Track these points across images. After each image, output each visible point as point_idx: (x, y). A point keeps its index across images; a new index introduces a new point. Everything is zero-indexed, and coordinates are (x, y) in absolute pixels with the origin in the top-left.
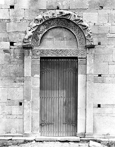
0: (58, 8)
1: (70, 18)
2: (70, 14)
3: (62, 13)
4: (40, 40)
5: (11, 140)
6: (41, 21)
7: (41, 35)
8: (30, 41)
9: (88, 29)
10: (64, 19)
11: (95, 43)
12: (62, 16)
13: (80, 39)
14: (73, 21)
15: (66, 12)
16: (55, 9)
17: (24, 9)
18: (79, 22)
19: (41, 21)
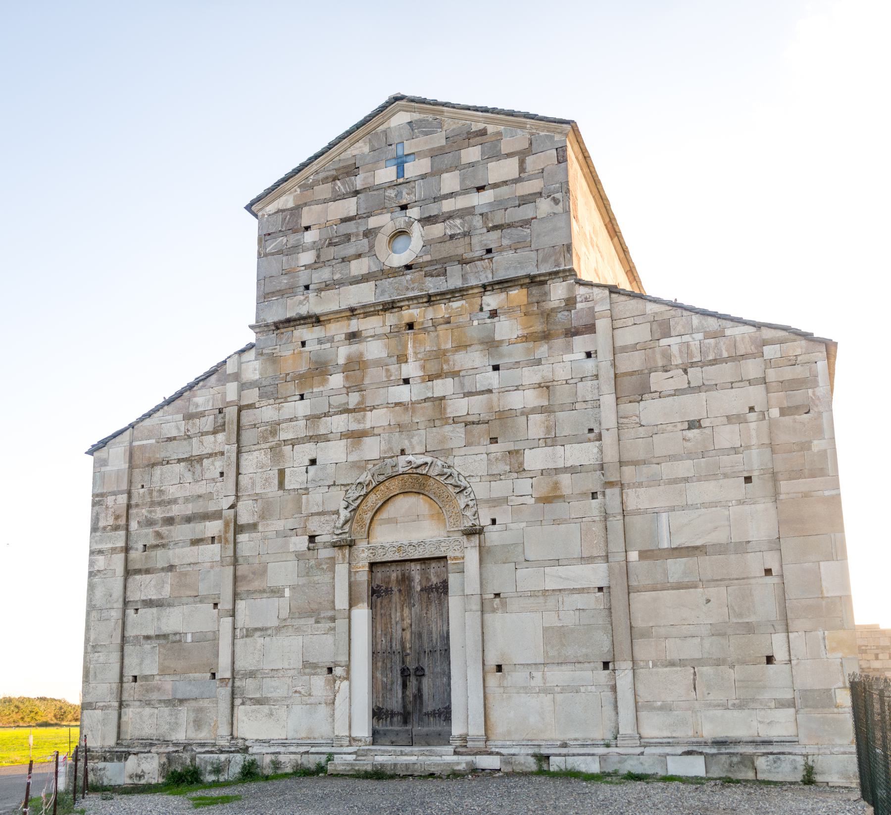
0: (403, 452)
1: (427, 472)
2: (426, 463)
3: (410, 462)
4: (368, 525)
5: (307, 753)
6: (368, 485)
7: (370, 514)
8: (347, 530)
9: (466, 493)
10: (417, 473)
11: (485, 521)
12: (411, 468)
13: (451, 514)
14: (435, 477)
15: (420, 460)
16: (397, 456)
17: (336, 463)
18: (445, 479)
19: (368, 485)
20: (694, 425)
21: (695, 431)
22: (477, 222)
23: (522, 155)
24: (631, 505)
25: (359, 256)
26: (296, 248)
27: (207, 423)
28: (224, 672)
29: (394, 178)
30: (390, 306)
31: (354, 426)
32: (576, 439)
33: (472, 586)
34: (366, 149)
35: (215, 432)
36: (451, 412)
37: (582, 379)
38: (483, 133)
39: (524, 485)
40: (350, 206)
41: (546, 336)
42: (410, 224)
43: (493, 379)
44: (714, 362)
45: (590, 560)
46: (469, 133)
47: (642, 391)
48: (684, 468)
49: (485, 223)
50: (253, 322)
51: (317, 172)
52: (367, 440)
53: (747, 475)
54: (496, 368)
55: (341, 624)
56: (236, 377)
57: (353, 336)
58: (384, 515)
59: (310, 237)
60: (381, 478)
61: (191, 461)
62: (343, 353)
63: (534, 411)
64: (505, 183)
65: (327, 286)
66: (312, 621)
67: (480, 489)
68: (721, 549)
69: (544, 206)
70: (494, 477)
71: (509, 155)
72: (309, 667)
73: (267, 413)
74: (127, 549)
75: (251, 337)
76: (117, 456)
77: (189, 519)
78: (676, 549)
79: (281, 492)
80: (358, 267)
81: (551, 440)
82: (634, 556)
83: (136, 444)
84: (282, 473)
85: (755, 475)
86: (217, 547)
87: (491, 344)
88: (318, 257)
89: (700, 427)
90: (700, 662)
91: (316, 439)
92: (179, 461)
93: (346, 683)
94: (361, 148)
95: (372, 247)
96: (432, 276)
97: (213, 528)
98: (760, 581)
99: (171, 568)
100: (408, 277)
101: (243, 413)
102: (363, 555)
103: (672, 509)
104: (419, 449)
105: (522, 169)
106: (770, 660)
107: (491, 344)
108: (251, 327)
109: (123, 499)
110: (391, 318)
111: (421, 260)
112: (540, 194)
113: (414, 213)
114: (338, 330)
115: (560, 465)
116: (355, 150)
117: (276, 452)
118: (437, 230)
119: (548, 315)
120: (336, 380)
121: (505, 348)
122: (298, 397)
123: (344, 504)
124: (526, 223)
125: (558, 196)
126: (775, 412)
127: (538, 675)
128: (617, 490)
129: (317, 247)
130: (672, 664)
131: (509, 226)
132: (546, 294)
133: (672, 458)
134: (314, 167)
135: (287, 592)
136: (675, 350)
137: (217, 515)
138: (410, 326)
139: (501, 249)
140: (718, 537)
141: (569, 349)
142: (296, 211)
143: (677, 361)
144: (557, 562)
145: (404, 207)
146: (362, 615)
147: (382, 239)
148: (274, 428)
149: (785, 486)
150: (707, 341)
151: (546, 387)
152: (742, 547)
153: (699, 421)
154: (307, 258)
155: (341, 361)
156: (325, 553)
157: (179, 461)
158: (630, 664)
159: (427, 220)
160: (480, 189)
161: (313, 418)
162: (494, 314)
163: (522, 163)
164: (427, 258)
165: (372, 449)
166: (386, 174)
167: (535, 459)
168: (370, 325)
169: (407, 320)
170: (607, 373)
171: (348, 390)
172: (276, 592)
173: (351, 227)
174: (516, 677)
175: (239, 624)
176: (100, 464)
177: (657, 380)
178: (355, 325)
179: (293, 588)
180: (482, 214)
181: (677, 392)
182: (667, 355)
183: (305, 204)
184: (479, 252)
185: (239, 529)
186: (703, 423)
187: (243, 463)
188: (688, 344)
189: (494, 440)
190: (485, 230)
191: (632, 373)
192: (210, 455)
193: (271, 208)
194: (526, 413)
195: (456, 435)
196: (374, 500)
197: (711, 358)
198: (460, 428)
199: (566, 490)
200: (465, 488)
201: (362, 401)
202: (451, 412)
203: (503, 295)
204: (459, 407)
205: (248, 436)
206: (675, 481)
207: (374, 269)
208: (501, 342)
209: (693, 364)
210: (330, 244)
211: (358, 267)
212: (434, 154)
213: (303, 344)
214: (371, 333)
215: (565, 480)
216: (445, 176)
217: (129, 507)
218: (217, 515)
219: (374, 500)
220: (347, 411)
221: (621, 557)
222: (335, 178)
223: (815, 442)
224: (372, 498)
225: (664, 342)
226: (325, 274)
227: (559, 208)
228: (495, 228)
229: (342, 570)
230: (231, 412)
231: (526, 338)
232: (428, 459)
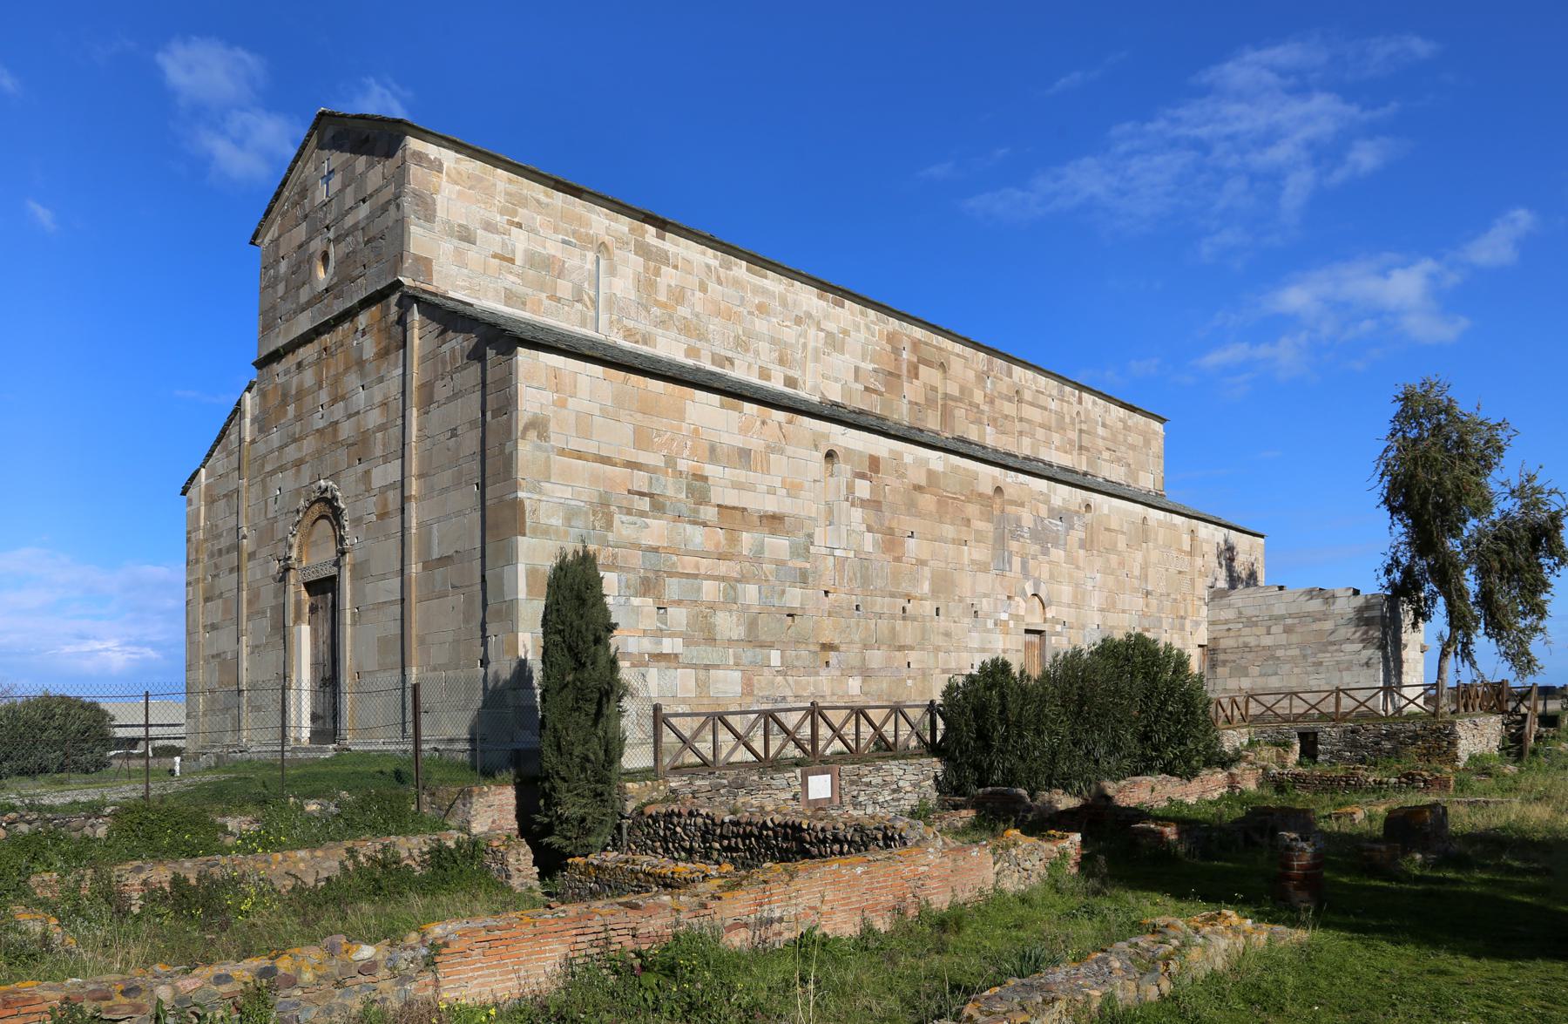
118: (344, 248)
159: (337, 240)
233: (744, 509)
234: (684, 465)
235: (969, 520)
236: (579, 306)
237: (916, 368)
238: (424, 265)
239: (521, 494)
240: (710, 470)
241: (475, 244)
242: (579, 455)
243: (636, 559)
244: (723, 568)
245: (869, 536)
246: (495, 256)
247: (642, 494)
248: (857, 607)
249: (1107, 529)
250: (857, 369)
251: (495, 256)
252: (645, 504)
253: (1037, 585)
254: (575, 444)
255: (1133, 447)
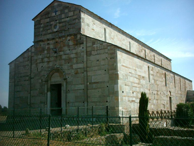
0: (55, 65)
20: (98, 60)
21: (98, 62)
22: (67, 23)
23: (74, 11)
24: (88, 74)
25: (49, 29)
26: (40, 27)
27: (26, 59)
28: (29, 104)
29: (55, 15)
30: (53, 39)
31: (48, 60)
32: (81, 63)
33: (65, 89)
34: (51, 9)
35: (28, 61)
36: (63, 58)
37: (82, 52)
38: (68, 7)
39: (73, 71)
40: (48, 20)
41: (77, 45)
42: (57, 24)
43: (68, 52)
44: (101, 49)
45: (82, 84)
46: (66, 7)
47: (91, 54)
48: (96, 68)
49: (68, 24)
50: (33, 41)
51: (43, 13)
52: (50, 63)
53: (105, 69)
54: (69, 50)
55: (46, 95)
56: (31, 51)
57: (48, 44)
58: (53, 76)
59: (42, 25)
60: (52, 69)
61: (24, 66)
62: (47, 47)
63: (75, 58)
64: (71, 16)
65: (45, 35)
66: (42, 94)
67: (66, 72)
68: (101, 82)
69: (77, 20)
70: (69, 69)
71: (72, 11)
72: (41, 102)
73: (35, 58)
74: (15, 82)
75: (33, 44)
76: (13, 65)
77: (24, 76)
78: (94, 82)
79: (37, 72)
80: (49, 31)
81: (77, 63)
82: (88, 83)
83: (16, 63)
84: (37, 68)
85: (106, 69)
86: (28, 82)
87: (69, 46)
88: (43, 29)
89: (98, 61)
90: (97, 102)
91: (43, 62)
92: (22, 66)
93: (46, 105)
94: (50, 9)
95: (51, 27)
96: (60, 33)
97: (27, 78)
98: (106, 88)
99: (21, 85)
100: (57, 33)
101: (32, 57)
102: (49, 84)
103: (94, 75)
104: (58, 65)
105: (74, 14)
106: (107, 102)
107: (69, 46)
108: (33, 42)
109: (14, 73)
110: (54, 41)
111: (58, 30)
112: (76, 18)
113: (58, 21)
114: (46, 43)
115: (78, 68)
116: (49, 10)
117: (37, 64)
118: (61, 25)
119: (77, 41)
120: (46, 52)
121: (71, 47)
122: (40, 55)
123: (46, 74)
124: (74, 24)
125: (79, 19)
126: (109, 59)
127: (74, 104)
128: (86, 72)
129: (43, 27)
130: (93, 102)
131: (72, 24)
132: (77, 37)
133: (95, 66)
134: (42, 13)
135: (38, 90)
136: (95, 47)
137: (28, 76)
138: (57, 42)
139: (70, 28)
140: (101, 80)
141: (80, 47)
142: (40, 21)
143: (96, 49)
144: (77, 85)
145: (56, 20)
146: (49, 94)
147: (53, 26)
148: (36, 60)
149: (110, 72)
150: (100, 46)
151: (76, 54)
152: (104, 82)
153: (98, 60)
154: (41, 29)
155: (46, 49)
156: (44, 83)
157: (22, 66)
158: (86, 102)
159: (60, 23)
160: (68, 17)
161: (42, 59)
162: (69, 40)
163: (74, 13)
164: (60, 30)
165: (51, 64)
166: (54, 14)
167: (75, 66)
168: (51, 42)
169: (56, 41)
170: (85, 51)
171: (47, 53)
172: (37, 90)
173: (48, 24)
174: (71, 104)
175: (31, 95)
176: (10, 67)
177: (93, 52)
178: (48, 42)
179: (39, 89)
180: (68, 22)
181: (96, 55)
182: (94, 48)
183: (41, 19)
184: (67, 29)
185: (31, 78)
186: (99, 60)
187: (32, 67)
188: (97, 46)
189: (69, 63)
190: (68, 25)
191: (89, 51)
192: (27, 65)
193: (36, 20)
194: (73, 58)
195: (63, 62)
196: (51, 73)
197: (101, 49)
198: (64, 61)
199: (79, 72)
200: (64, 71)
201: (49, 56)
202: (63, 58)
203: (71, 37)
204: (64, 57)
205: (32, 62)
206: (94, 71)
207: (52, 32)
208: (70, 45)
209: (98, 50)
210: (45, 27)
211: (49, 31)
212: (61, 11)
213: (41, 45)
214: (51, 43)
215: (79, 70)
216: (62, 15)
217: (15, 74)
218: (28, 76)
219: (51, 73)
220: (47, 57)
221: (86, 84)
222: (46, 15)
223: (115, 64)
224: (51, 73)
225: (94, 46)
226: (44, 33)
227: (79, 21)
228: (70, 24)
229: (46, 86)
230: (30, 57)
231: (74, 45)
232: (59, 66)
233: (140, 76)
234: (134, 68)
235: (162, 78)
236: (102, 38)
237: (142, 50)
238: (84, 29)
239: (118, 73)
240: (137, 69)
241: (89, 27)
242: (124, 66)
243: (130, 84)
244: (139, 86)
245: (153, 80)
246: (92, 29)
247: (130, 73)
248: (152, 93)
249: (177, 80)
250: (135, 50)
251: (92, 29)
252: (130, 74)
253: (170, 89)
254: (124, 64)
255: (168, 65)
